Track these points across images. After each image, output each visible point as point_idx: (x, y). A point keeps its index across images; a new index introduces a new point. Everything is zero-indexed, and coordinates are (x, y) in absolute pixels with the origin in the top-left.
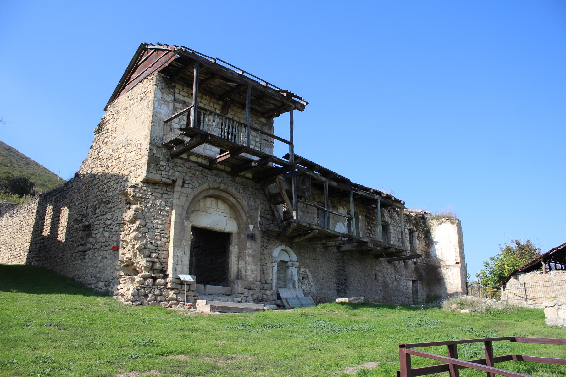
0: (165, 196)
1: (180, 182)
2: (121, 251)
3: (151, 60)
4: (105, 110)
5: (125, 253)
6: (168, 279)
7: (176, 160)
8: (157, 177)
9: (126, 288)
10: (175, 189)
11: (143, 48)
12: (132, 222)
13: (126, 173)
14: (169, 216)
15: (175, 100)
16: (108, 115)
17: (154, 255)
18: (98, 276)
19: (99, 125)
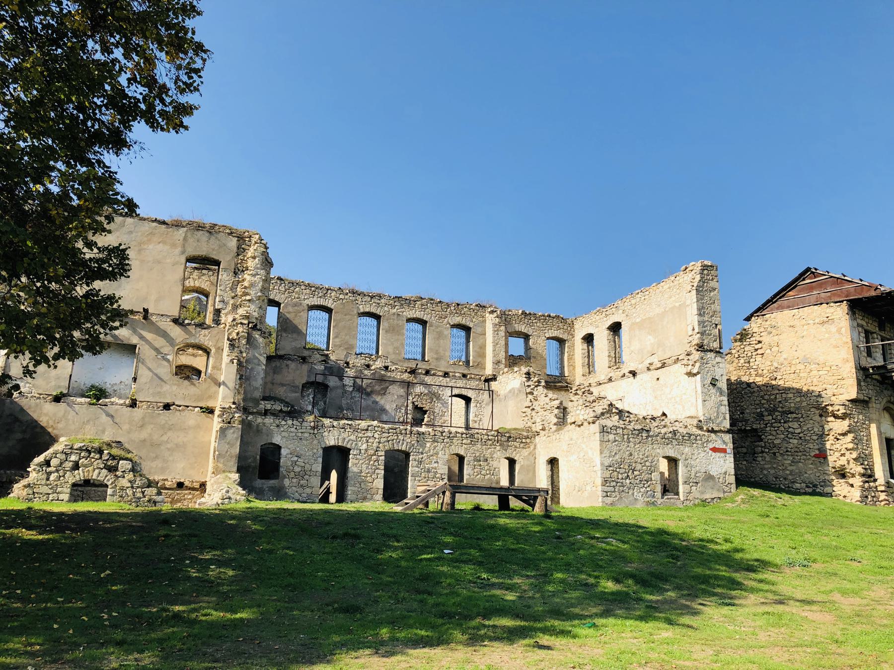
0: (864, 412)
1: (873, 398)
2: (831, 459)
3: (822, 284)
4: (748, 319)
5: (834, 460)
6: (877, 483)
7: (868, 380)
8: (861, 397)
9: (848, 492)
10: (870, 405)
11: (807, 272)
12: (844, 434)
13: (817, 389)
14: (868, 429)
15: (858, 325)
16: (755, 325)
17: (866, 463)
18: (790, 477)
19: (741, 334)
